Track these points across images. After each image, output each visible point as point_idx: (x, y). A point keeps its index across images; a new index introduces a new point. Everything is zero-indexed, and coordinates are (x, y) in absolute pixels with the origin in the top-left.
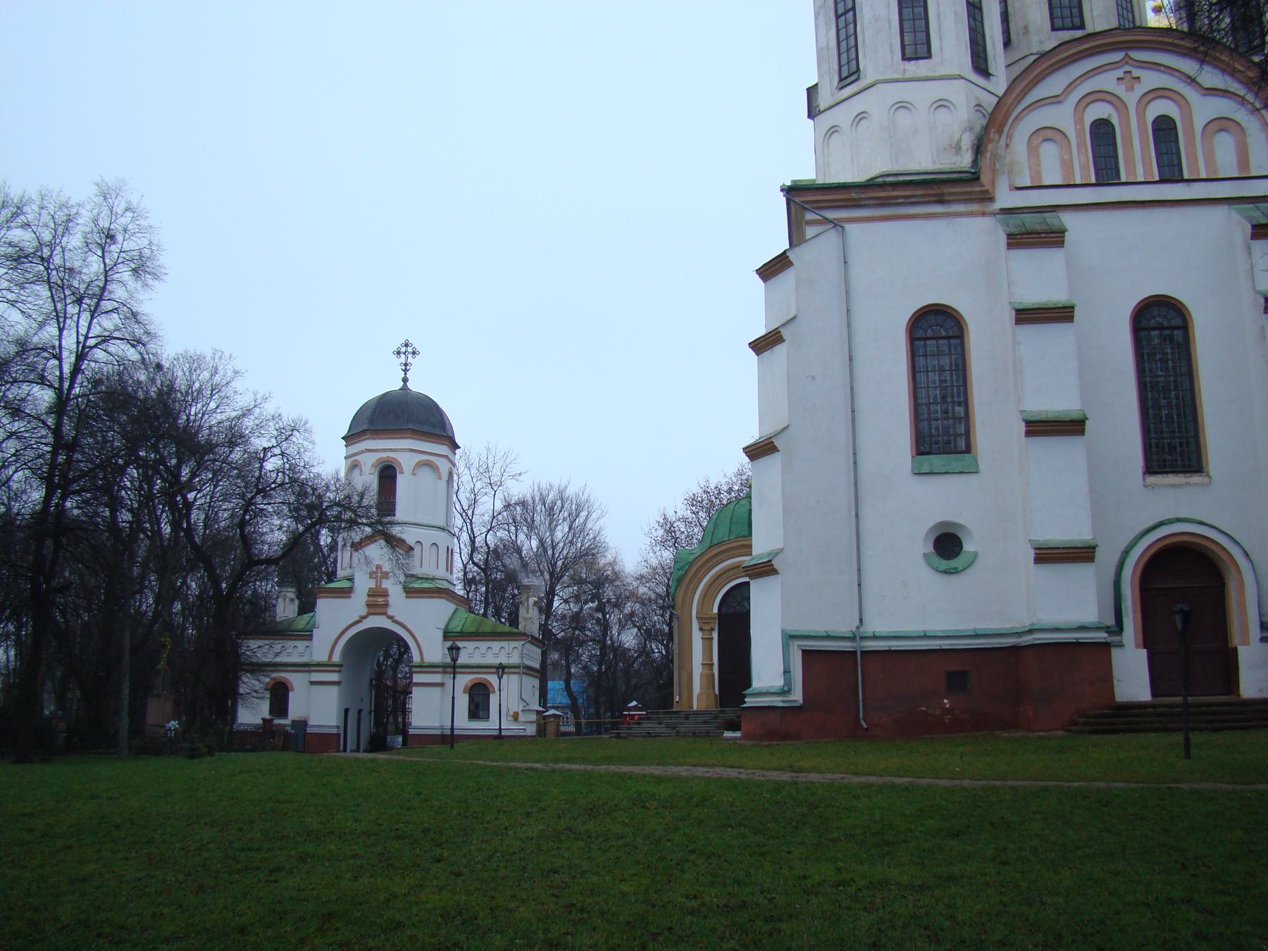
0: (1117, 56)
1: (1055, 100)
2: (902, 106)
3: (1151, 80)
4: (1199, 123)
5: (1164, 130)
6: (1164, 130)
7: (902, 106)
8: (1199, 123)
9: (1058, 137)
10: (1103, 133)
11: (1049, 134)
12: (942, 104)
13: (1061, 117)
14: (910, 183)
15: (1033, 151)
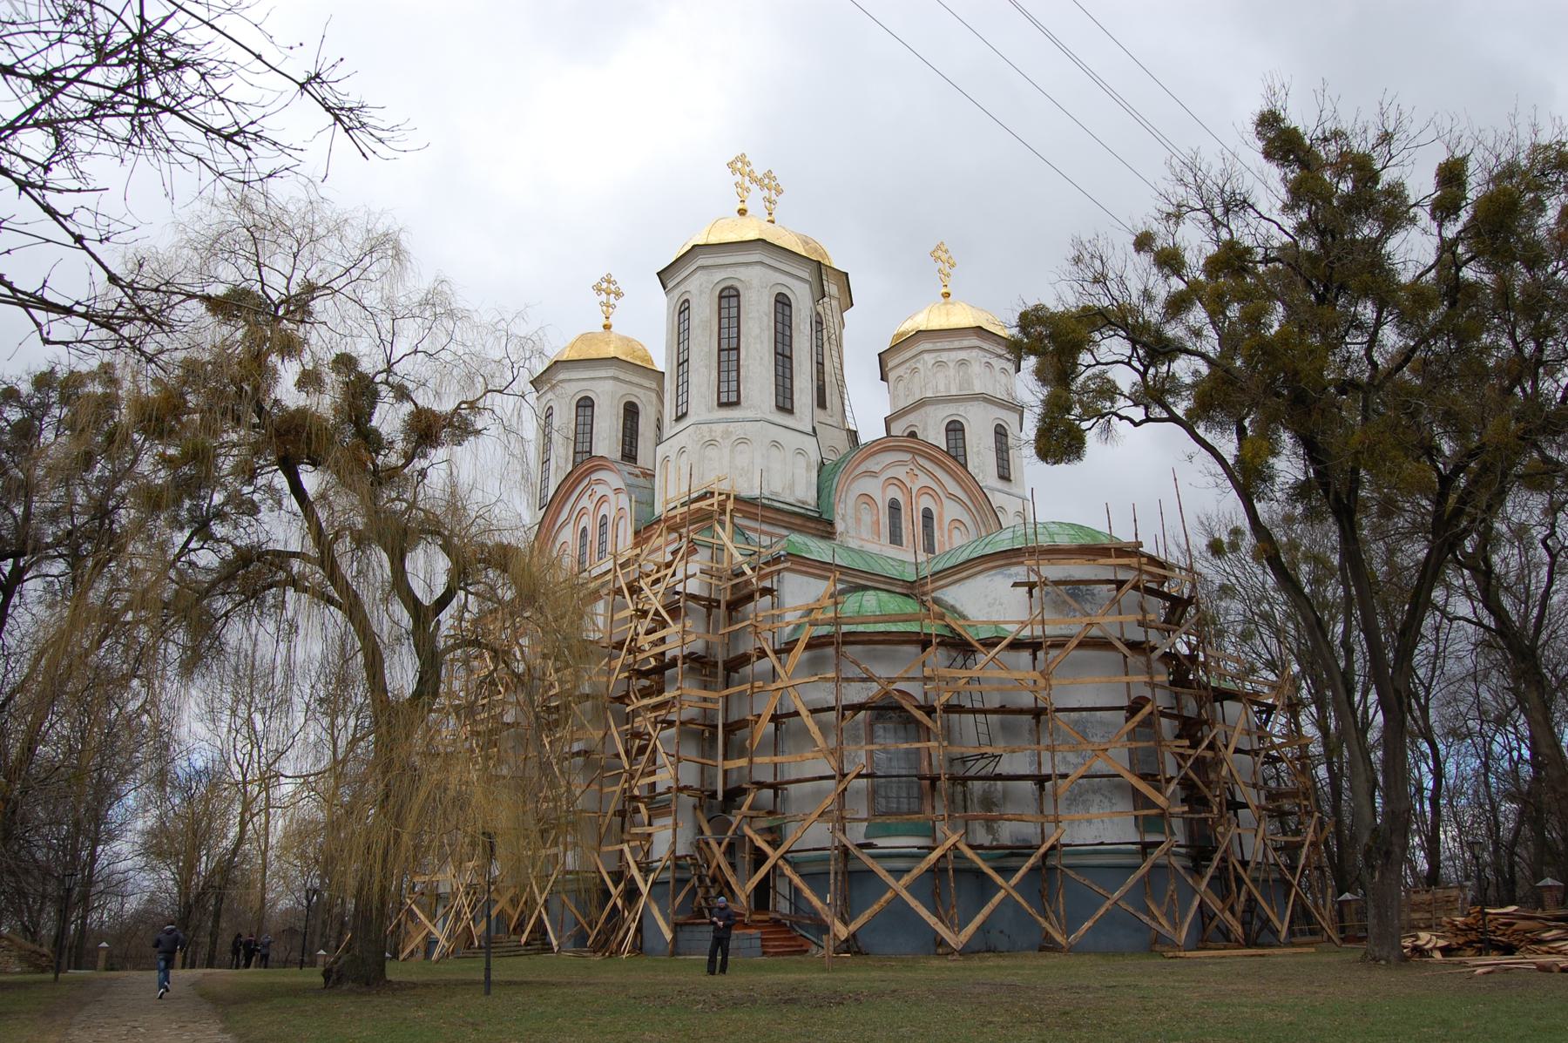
0: (907, 457)
1: (873, 474)
2: (776, 444)
3: (924, 480)
4: (947, 520)
5: (928, 515)
6: (928, 515)
7: (776, 444)
8: (947, 520)
9: (962, 528)
10: (894, 507)
11: (869, 500)
12: (800, 452)
13: (872, 486)
14: (778, 510)
15: (857, 510)
